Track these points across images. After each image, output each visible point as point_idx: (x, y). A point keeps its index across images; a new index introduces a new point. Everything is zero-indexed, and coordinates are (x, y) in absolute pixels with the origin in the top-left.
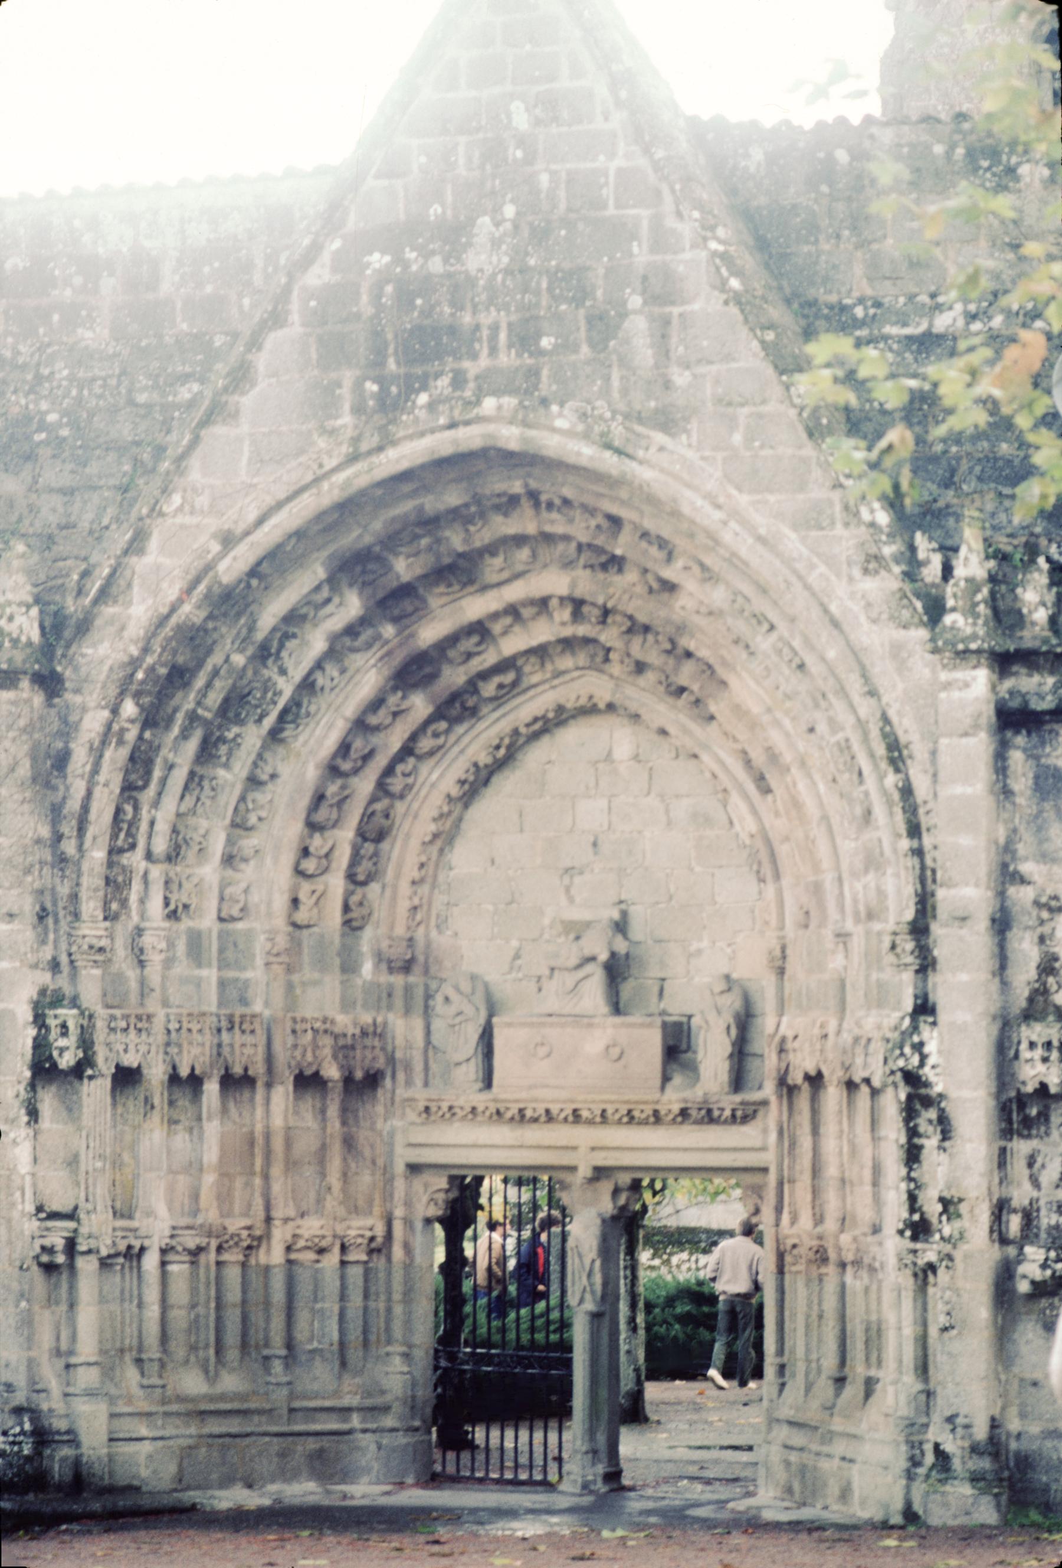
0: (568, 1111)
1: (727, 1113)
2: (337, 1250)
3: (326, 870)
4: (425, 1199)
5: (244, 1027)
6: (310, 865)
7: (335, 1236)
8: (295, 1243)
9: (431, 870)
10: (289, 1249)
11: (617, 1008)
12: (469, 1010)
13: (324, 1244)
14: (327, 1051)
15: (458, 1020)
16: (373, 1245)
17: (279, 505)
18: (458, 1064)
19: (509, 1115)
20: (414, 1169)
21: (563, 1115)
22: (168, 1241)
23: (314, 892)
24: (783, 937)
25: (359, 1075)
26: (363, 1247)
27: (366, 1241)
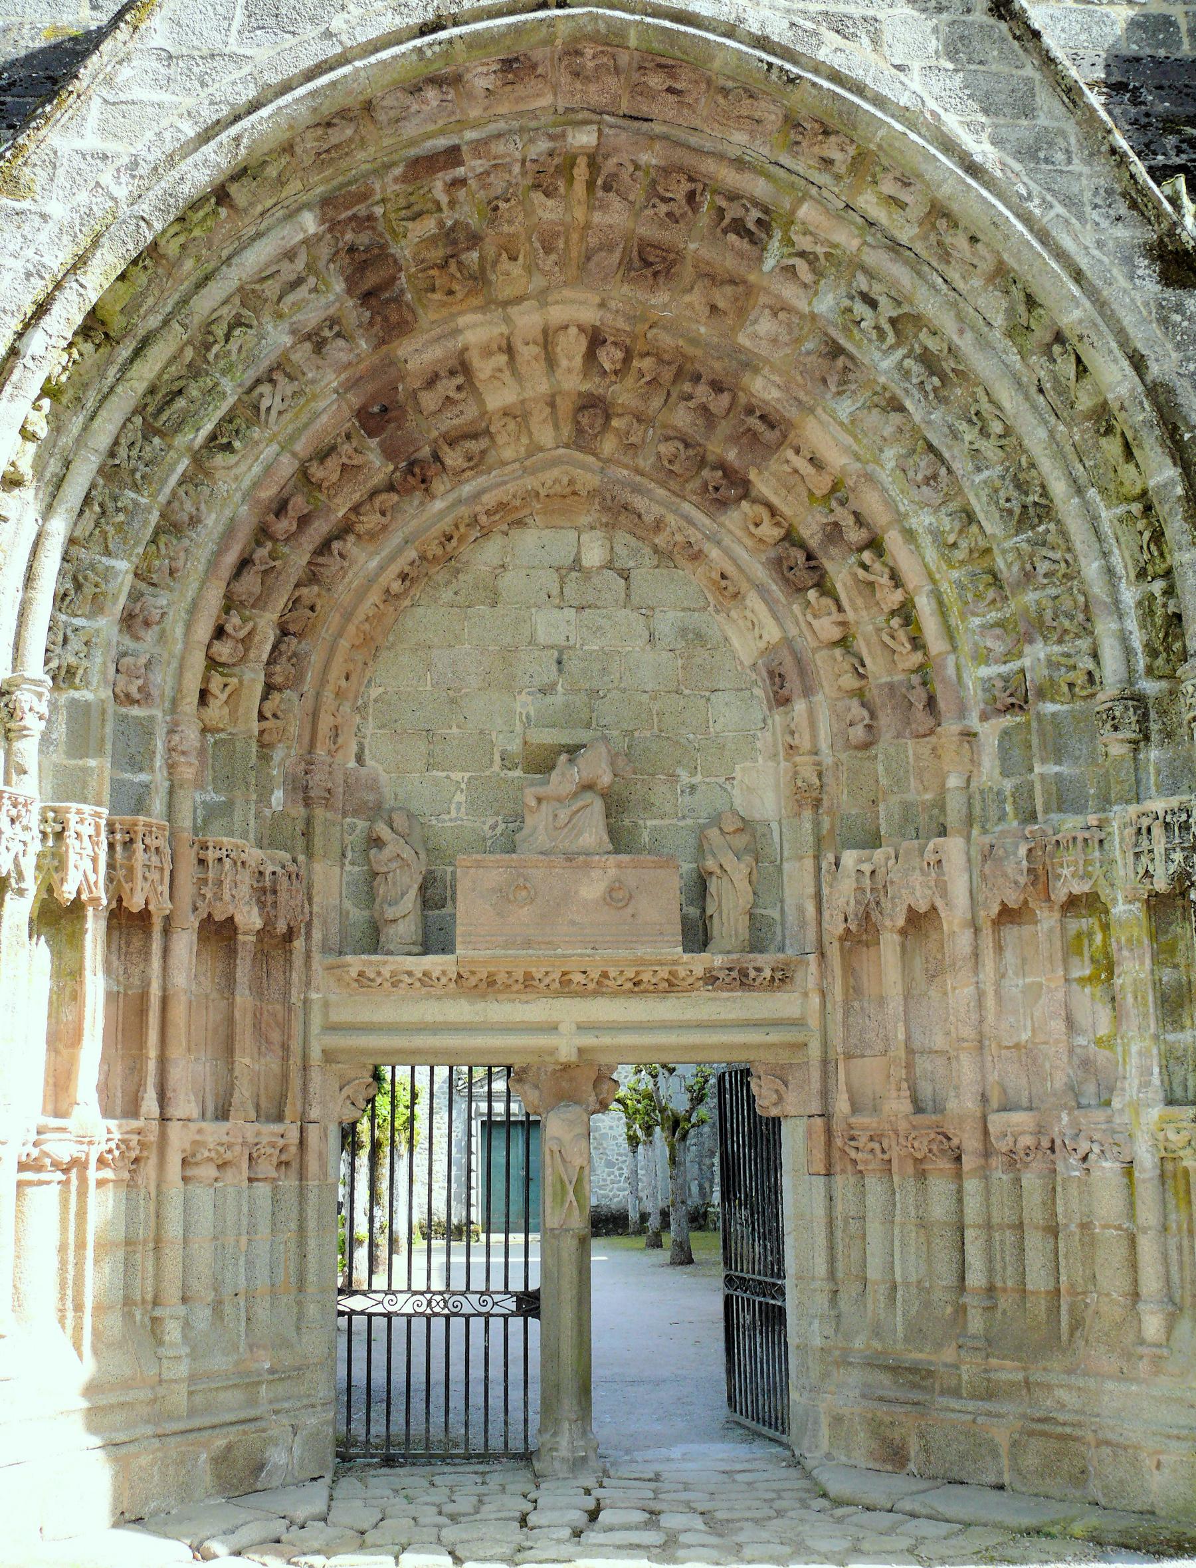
0: (557, 976)
1: (767, 973)
2: (245, 1165)
5: (148, 841)
6: (223, 650)
7: (244, 1144)
8: (194, 1155)
10: (185, 1162)
12: (407, 853)
13: (228, 1156)
14: (244, 891)
15: (394, 865)
16: (284, 1158)
17: (286, 88)
19: (473, 981)
20: (329, 1056)
21: (546, 981)
22: (29, 1148)
23: (226, 685)
24: (819, 764)
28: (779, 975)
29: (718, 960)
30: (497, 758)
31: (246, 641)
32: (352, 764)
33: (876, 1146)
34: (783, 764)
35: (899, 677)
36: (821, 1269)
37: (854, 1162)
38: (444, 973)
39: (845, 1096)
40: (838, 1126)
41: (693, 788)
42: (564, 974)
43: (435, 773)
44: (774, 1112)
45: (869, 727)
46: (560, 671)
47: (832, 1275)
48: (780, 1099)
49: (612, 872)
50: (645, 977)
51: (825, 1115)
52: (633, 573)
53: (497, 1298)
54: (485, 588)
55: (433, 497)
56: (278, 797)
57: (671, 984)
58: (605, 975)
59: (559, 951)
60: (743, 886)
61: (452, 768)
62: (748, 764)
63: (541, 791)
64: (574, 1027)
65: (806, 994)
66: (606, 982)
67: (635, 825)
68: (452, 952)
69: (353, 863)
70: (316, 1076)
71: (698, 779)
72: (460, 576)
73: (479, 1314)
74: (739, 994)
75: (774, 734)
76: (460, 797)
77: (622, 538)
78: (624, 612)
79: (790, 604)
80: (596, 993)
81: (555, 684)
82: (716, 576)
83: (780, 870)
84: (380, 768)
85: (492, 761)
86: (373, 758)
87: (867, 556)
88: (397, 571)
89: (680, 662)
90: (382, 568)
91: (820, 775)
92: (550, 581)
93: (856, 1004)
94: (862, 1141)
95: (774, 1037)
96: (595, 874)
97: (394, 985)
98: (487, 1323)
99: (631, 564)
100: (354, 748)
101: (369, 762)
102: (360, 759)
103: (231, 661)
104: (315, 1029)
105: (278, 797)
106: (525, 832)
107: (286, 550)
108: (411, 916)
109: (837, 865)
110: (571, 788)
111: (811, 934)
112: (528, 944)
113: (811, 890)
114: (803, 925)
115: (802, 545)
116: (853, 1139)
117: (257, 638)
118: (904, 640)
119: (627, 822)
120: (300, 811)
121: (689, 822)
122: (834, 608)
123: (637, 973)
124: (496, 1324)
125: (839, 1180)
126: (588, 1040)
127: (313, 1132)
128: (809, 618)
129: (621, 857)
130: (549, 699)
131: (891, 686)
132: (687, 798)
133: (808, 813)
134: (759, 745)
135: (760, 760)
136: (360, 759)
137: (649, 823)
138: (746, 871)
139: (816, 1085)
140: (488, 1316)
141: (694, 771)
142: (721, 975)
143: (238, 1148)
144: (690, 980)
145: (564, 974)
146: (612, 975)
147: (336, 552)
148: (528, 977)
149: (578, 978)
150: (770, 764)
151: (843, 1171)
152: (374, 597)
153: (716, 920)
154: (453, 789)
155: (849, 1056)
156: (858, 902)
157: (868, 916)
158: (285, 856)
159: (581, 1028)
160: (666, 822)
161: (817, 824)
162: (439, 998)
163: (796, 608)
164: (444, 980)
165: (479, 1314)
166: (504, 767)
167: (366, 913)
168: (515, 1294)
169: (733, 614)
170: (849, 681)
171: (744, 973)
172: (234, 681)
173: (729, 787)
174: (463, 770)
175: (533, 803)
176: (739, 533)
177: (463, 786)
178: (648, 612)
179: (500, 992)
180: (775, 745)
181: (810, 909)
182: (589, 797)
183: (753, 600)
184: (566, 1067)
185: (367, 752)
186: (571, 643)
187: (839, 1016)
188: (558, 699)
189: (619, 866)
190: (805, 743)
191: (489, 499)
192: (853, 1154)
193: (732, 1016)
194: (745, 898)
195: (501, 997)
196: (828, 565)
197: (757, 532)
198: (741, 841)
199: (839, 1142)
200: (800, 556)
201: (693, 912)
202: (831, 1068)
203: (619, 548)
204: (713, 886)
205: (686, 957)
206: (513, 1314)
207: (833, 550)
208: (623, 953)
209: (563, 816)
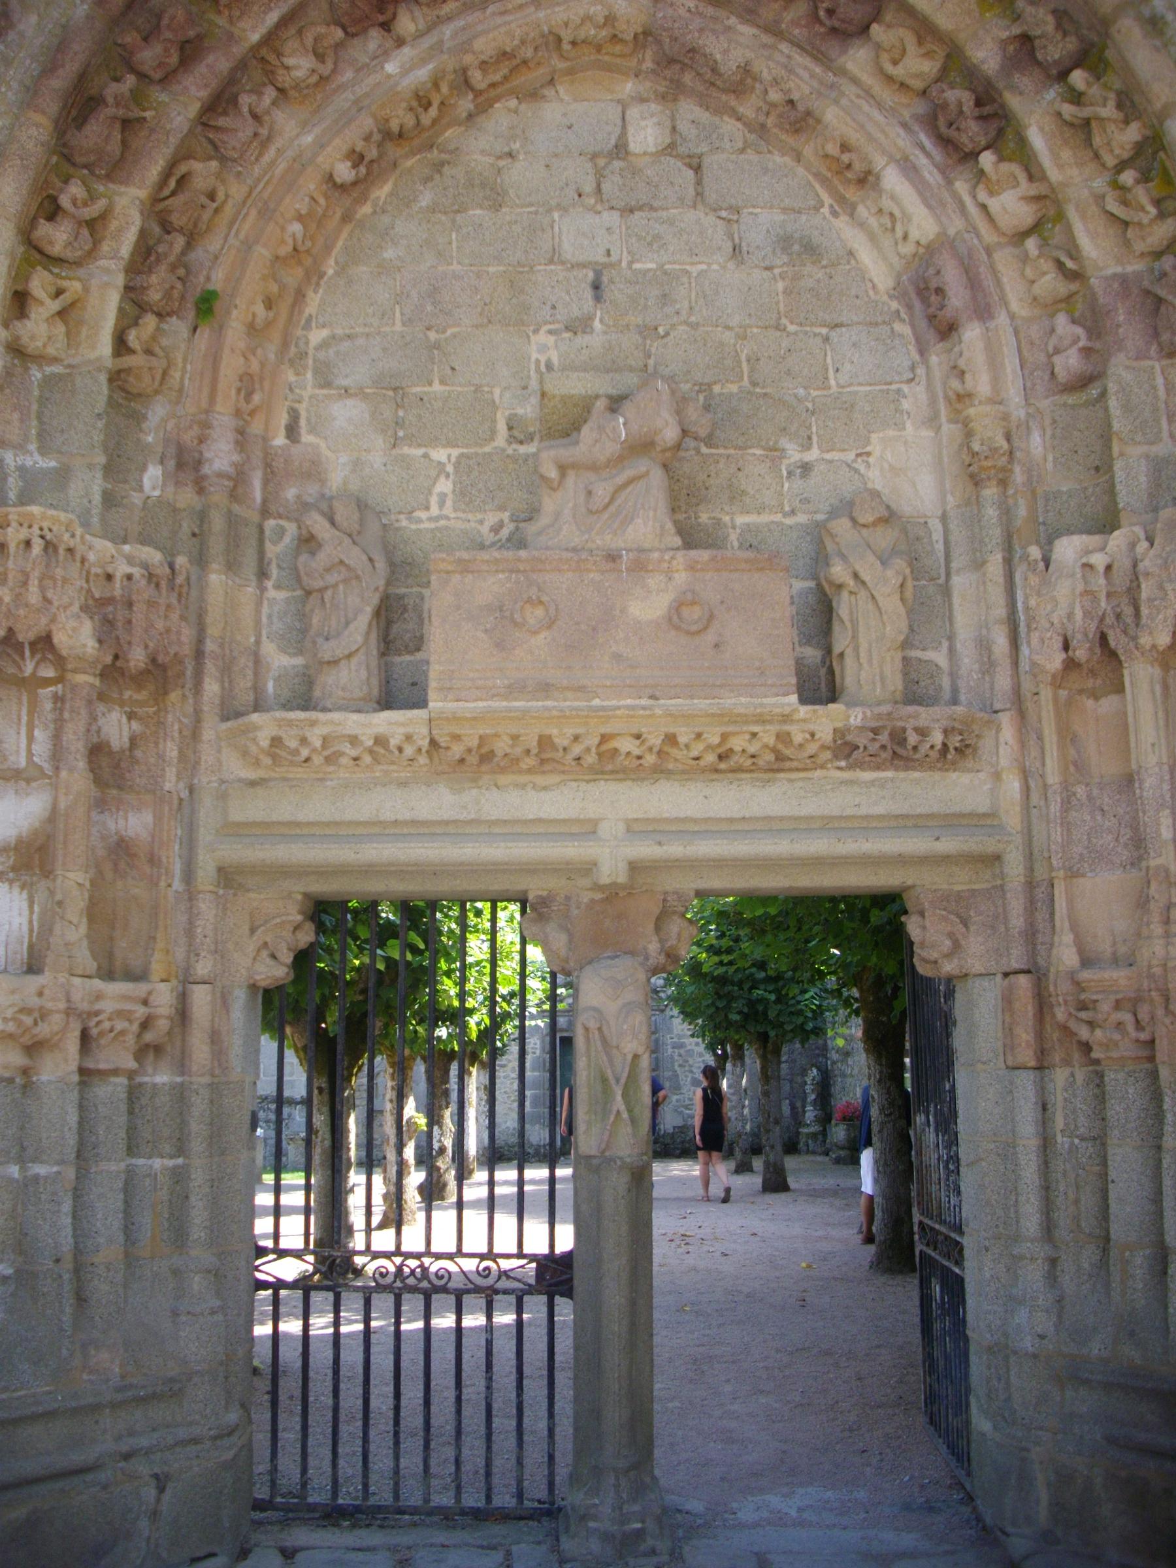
1: (937, 738)
3: (92, 254)
4: (251, 946)
7: (69, 1012)
9: (284, 308)
11: (691, 537)
12: (355, 558)
13: (44, 1030)
15: (331, 579)
16: (148, 1037)
18: (335, 663)
19: (457, 750)
21: (577, 750)
25: (137, 657)
26: (130, 1039)
27: (135, 1027)
28: (955, 741)
29: (856, 718)
30: (502, 427)
31: (95, 226)
32: (280, 440)
33: (1127, 1018)
34: (947, 428)
35: (1135, 267)
36: (1031, 1223)
37: (1086, 1047)
38: (409, 738)
39: (1068, 938)
40: (1060, 989)
41: (806, 468)
42: (604, 738)
43: (406, 450)
44: (948, 968)
45: (1087, 352)
46: (598, 298)
47: (1049, 1228)
48: (957, 946)
49: (681, 577)
50: (737, 743)
51: (1035, 971)
52: (706, 161)
53: (506, 1264)
54: (483, 185)
55: (400, 42)
56: (153, 476)
57: (780, 758)
58: (671, 739)
59: (596, 702)
60: (891, 604)
61: (434, 442)
62: (891, 433)
63: (566, 453)
64: (621, 827)
65: (997, 776)
66: (674, 752)
67: (718, 522)
68: (422, 703)
69: (278, 587)
70: (206, 908)
71: (813, 455)
72: (446, 169)
74: (889, 774)
75: (930, 387)
76: (444, 486)
77: (689, 111)
78: (691, 215)
79: (950, 183)
80: (659, 772)
81: (591, 318)
82: (832, 149)
83: (946, 591)
84: (323, 445)
85: (493, 432)
86: (312, 430)
87: (1078, 78)
88: (345, 148)
89: (780, 286)
90: (320, 145)
91: (1008, 437)
92: (581, 174)
93: (1080, 791)
94: (1105, 1007)
95: (948, 845)
96: (654, 581)
97: (328, 760)
99: (704, 148)
100: (283, 419)
101: (306, 438)
102: (292, 431)
103: (69, 255)
104: (205, 836)
105: (153, 476)
106: (544, 520)
107: (163, 97)
108: (361, 656)
109: (1047, 562)
110: (611, 448)
111: (1003, 681)
112: (545, 689)
113: (1000, 611)
114: (988, 666)
115: (971, 76)
116: (1083, 1006)
117: (114, 225)
118: (1144, 200)
119: (704, 518)
120: (187, 497)
121: (801, 518)
122: (1022, 177)
123: (724, 737)
125: (1060, 1076)
126: (646, 850)
127: (201, 997)
128: (982, 196)
129: (693, 553)
130: (581, 340)
131: (1123, 279)
132: (798, 483)
133: (990, 492)
134: (906, 405)
135: (908, 425)
136: (292, 431)
137: (741, 520)
138: (895, 581)
139: (1017, 921)
141: (807, 446)
142: (862, 741)
143: (57, 1020)
144: (812, 748)
145: (604, 738)
146: (682, 740)
147: (245, 110)
148: (545, 742)
149: (626, 745)
150: (927, 433)
151: (1067, 1062)
152: (311, 184)
153: (849, 661)
154: (433, 473)
155: (1073, 874)
156: (1086, 614)
157: (1103, 639)
158: (154, 556)
159: (635, 828)
160: (765, 518)
161: (1006, 513)
162: (403, 784)
163: (961, 187)
164: (409, 751)
166: (512, 439)
167: (299, 661)
168: (533, 1258)
169: (862, 211)
170: (1050, 283)
171: (899, 738)
172: (74, 287)
173: (862, 469)
174: (450, 444)
175: (553, 474)
176: (867, 79)
177: (450, 469)
178: (731, 214)
179: (503, 770)
180: (933, 402)
181: (1001, 641)
182: (643, 465)
183: (892, 179)
184: (612, 894)
185: (303, 422)
186: (614, 258)
187: (1055, 808)
188: (596, 339)
189: (691, 567)
190: (982, 385)
191: (485, 46)
192: (1084, 1033)
193: (880, 810)
194: (896, 624)
195: (503, 780)
196: (1013, 102)
197: (897, 72)
198: (884, 538)
199: (1060, 1014)
200: (967, 98)
201: (812, 654)
202: (1040, 893)
203: (683, 126)
204: (843, 607)
205: (804, 711)
207: (1024, 81)
208: (701, 704)
209: (602, 491)
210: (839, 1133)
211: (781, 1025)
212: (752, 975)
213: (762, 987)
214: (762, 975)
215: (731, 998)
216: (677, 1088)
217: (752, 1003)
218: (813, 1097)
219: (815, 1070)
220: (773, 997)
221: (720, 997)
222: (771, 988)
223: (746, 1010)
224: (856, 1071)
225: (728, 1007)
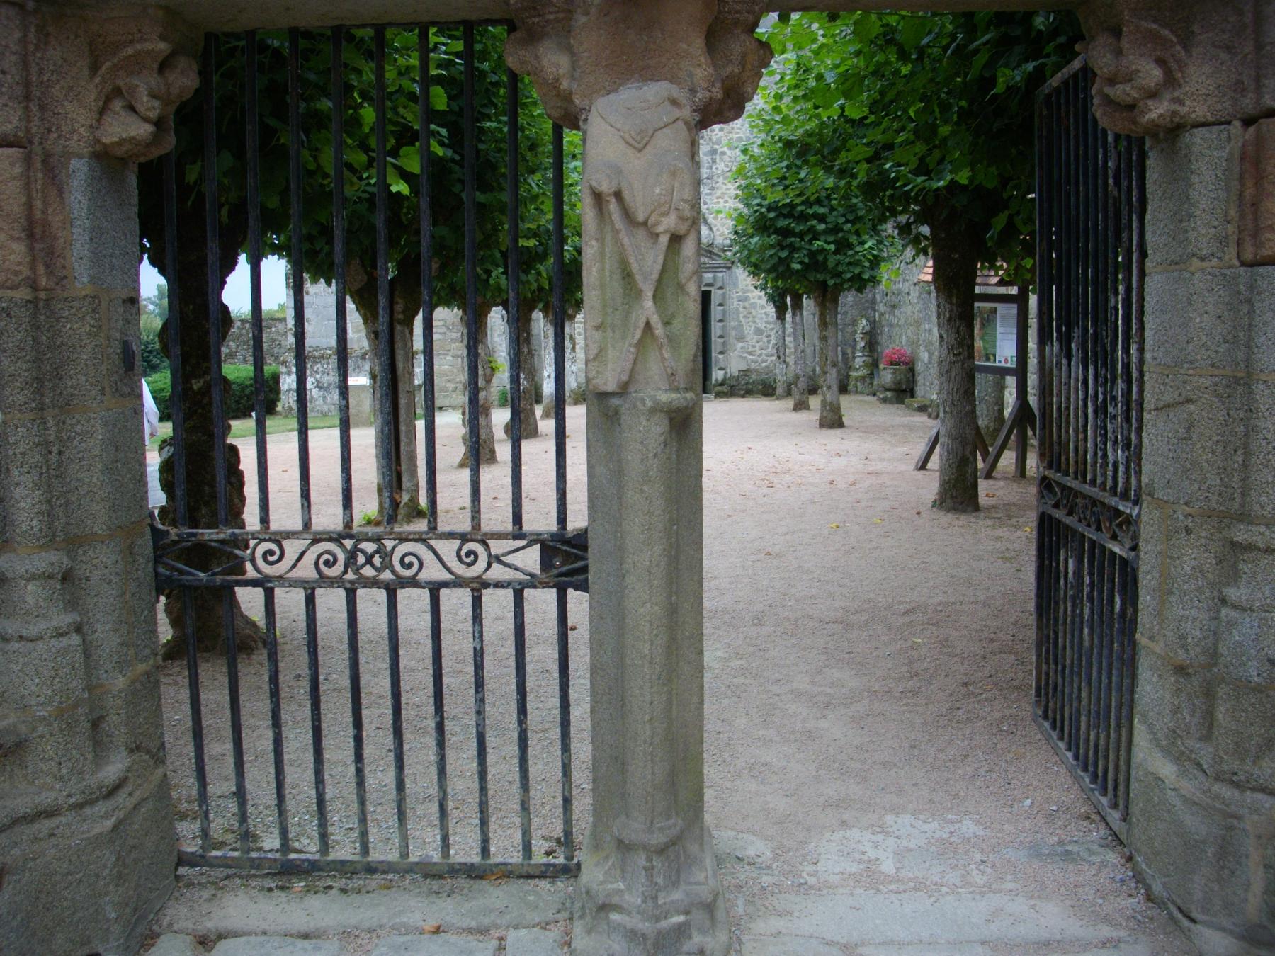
53: (497, 547)
73: (458, 583)
98: (477, 602)
124: (498, 604)
140: (478, 587)
165: (458, 583)
168: (534, 539)
206: (533, 582)
210: (887, 376)
211: (839, 275)
212: (813, 227)
213: (823, 238)
214: (822, 227)
215: (793, 249)
216: (741, 338)
217: (812, 254)
218: (863, 344)
219: (864, 321)
220: (832, 247)
221: (782, 248)
222: (831, 238)
223: (806, 260)
224: (901, 322)
225: (790, 257)
